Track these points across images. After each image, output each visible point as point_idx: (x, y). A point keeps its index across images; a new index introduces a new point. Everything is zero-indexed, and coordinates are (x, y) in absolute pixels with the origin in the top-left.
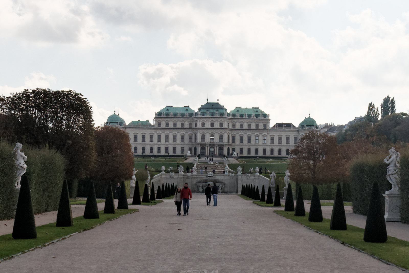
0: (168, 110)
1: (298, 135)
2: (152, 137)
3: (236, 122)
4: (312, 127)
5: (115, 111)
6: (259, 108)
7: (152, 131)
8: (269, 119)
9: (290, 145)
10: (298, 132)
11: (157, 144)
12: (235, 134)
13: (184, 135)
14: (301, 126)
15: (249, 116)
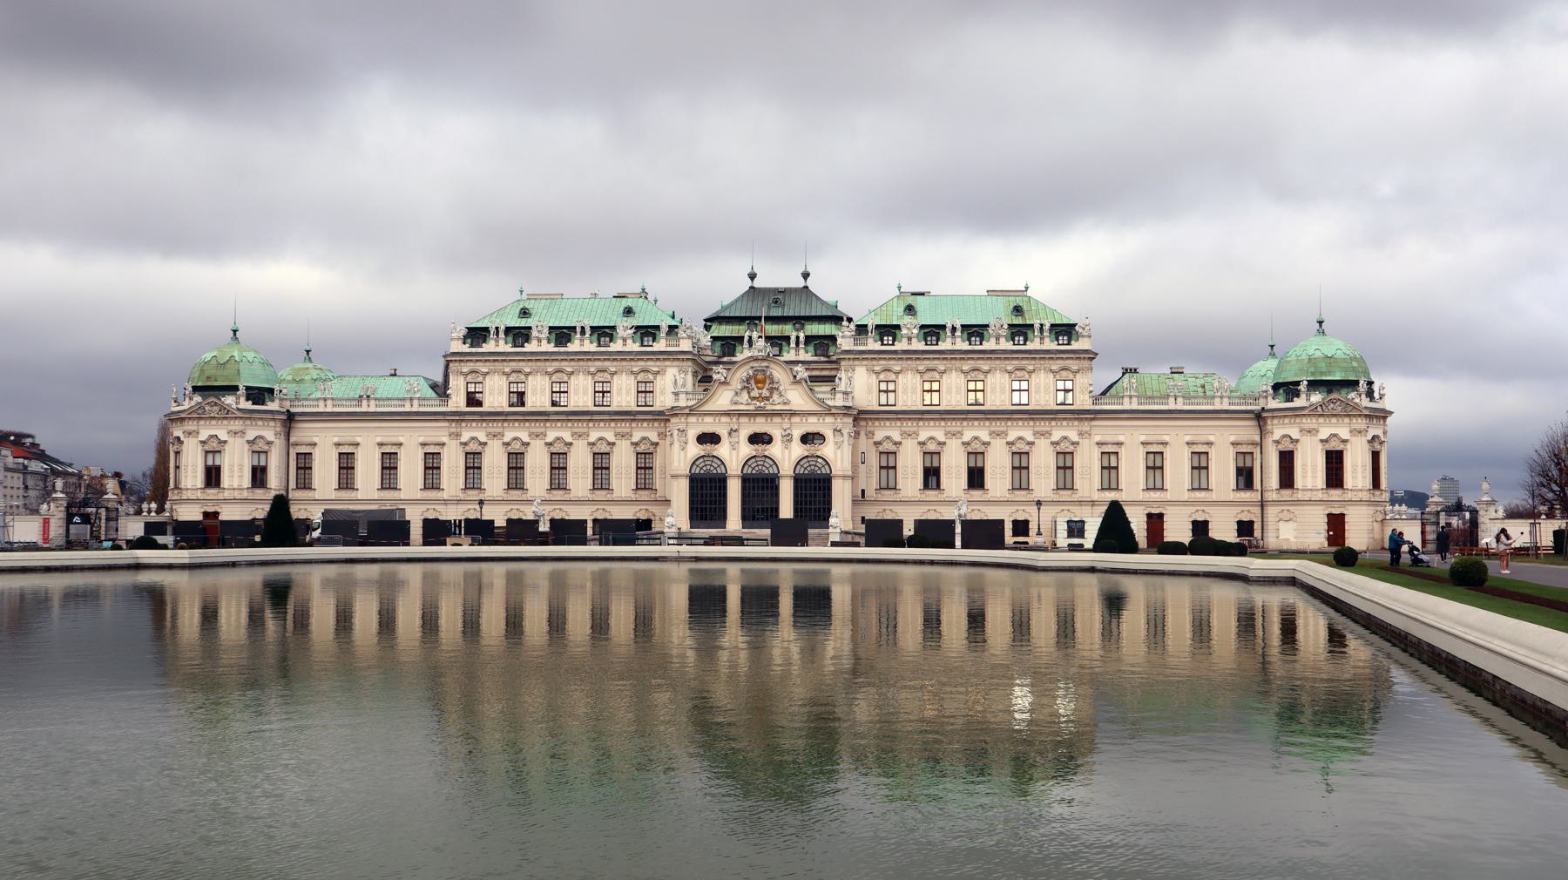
0: (525, 313)
1: (1257, 438)
2: (432, 465)
3: (897, 373)
4: (1344, 392)
5: (238, 325)
6: (1029, 293)
7: (437, 433)
8: (1086, 351)
9: (1214, 496)
10: (1254, 423)
11: (459, 502)
12: (897, 437)
13: (607, 449)
14: (1276, 387)
15: (975, 331)
